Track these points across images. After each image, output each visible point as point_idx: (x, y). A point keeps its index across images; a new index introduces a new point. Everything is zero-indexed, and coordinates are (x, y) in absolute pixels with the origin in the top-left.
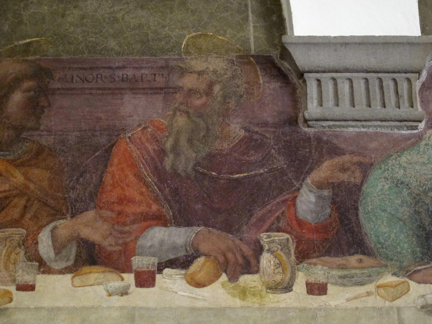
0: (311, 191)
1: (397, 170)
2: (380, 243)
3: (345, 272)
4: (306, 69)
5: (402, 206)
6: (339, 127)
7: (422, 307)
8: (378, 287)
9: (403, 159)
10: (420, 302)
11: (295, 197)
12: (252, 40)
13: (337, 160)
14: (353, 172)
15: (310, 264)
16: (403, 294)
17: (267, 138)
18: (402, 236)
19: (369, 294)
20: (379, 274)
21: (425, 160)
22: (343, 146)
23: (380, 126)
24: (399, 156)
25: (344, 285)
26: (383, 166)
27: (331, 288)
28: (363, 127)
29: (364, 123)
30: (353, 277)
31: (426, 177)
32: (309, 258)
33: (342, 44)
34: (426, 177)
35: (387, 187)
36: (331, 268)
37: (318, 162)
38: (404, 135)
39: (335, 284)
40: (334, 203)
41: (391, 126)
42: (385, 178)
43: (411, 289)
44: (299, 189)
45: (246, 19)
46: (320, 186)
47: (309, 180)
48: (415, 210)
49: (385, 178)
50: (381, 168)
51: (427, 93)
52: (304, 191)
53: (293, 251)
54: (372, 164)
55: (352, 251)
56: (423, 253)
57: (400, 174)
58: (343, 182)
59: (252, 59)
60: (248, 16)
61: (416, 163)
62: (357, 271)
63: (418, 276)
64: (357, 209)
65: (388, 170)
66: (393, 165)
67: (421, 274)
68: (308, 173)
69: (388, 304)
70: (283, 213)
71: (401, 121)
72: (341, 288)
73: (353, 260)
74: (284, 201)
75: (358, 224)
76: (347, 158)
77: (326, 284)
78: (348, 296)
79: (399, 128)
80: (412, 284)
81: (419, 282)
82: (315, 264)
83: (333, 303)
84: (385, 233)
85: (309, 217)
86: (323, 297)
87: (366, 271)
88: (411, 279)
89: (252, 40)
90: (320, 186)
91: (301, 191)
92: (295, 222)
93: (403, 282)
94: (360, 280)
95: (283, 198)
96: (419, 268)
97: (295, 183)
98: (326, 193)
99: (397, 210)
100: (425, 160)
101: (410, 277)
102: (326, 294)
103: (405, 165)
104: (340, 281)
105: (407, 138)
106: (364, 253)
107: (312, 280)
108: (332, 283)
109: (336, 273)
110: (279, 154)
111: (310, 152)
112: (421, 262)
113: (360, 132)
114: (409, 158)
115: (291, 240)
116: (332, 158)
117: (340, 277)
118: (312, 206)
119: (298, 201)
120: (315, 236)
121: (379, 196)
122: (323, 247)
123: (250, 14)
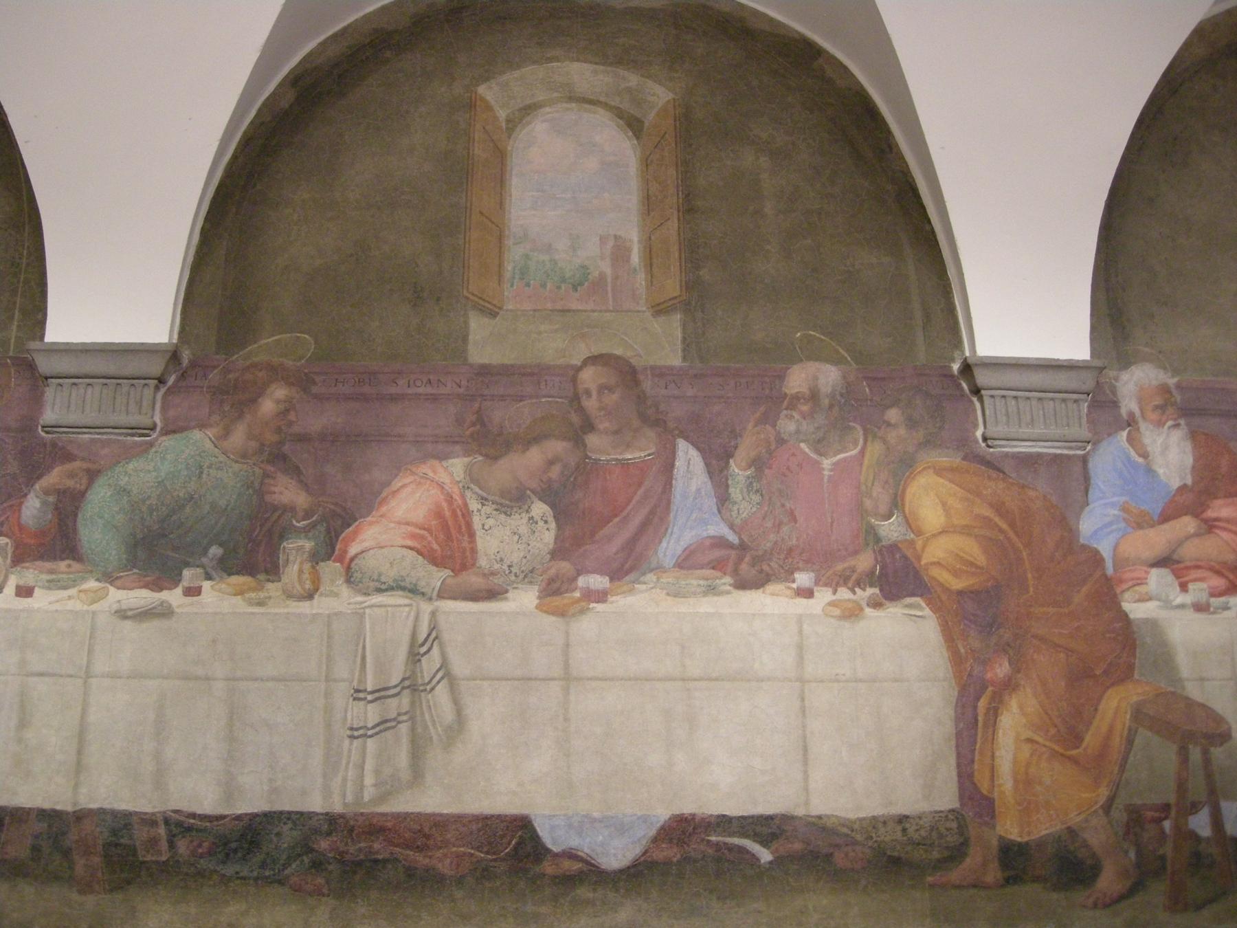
0: (37, 497)
1: (121, 477)
2: (90, 549)
3: (54, 576)
4: (48, 375)
5: (118, 513)
6: (73, 433)
7: (116, 612)
8: (80, 591)
9: (131, 466)
10: (115, 607)
11: (21, 504)
12: (13, 340)
13: (69, 466)
14: (80, 479)
15: (23, 568)
16: (101, 599)
17: (5, 443)
18: (113, 542)
19: (70, 598)
20: (84, 579)
21: (151, 468)
22: (76, 452)
23: (112, 433)
24: (127, 463)
25: (49, 588)
26: (109, 473)
27: (37, 592)
28: (98, 434)
29: (97, 430)
30: (59, 581)
31: (148, 484)
32: (23, 562)
33: (81, 351)
34: (148, 484)
35: (109, 494)
36: (41, 572)
37: (49, 468)
38: (136, 442)
39: (43, 587)
40: (56, 509)
41: (123, 434)
42: (109, 485)
43: (110, 594)
44: (26, 495)
45: (11, 318)
46: (47, 492)
47: (37, 486)
48: (131, 518)
49: (109, 485)
50: (107, 475)
51: (170, 398)
52: (31, 496)
53: (9, 555)
54: (99, 471)
55: (64, 556)
56: (127, 560)
57: (124, 481)
58: (69, 488)
59: (9, 361)
60: (14, 314)
61: (141, 471)
62: (64, 576)
63: (119, 583)
64: (76, 515)
65: (113, 476)
66: (119, 472)
67: (122, 580)
68: (39, 477)
69: (85, 607)
70: (8, 517)
71: (132, 429)
72: (47, 592)
73: (62, 565)
74: (11, 506)
75: (75, 530)
76: (77, 464)
77: (34, 587)
78: (53, 598)
79: (133, 435)
80: (112, 589)
81: (118, 588)
82: (27, 568)
83: (36, 606)
84: (97, 540)
85: (31, 523)
86: (29, 600)
87: (71, 576)
88: (112, 585)
89: (13, 340)
90: (47, 492)
91: (29, 496)
92: (16, 528)
93: (104, 588)
94: (65, 584)
95: (11, 503)
96: (122, 574)
97: (24, 488)
98: (51, 499)
99: (113, 517)
100: (151, 468)
101: (111, 583)
102: (32, 596)
103: (131, 472)
104: (46, 584)
105: (141, 444)
106: (74, 559)
107: (21, 583)
108: (39, 587)
109: (45, 577)
110: (14, 459)
111: (44, 458)
112: (125, 568)
113: (94, 439)
114: (136, 465)
115: (10, 544)
116: (63, 463)
117: (49, 581)
118: (35, 512)
119: (23, 507)
120: (32, 542)
121: (100, 503)
122: (38, 552)
123: (17, 312)
